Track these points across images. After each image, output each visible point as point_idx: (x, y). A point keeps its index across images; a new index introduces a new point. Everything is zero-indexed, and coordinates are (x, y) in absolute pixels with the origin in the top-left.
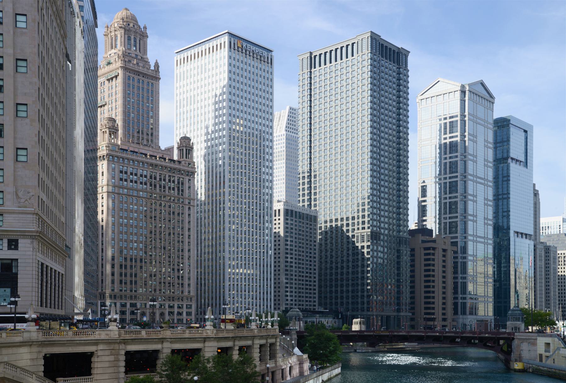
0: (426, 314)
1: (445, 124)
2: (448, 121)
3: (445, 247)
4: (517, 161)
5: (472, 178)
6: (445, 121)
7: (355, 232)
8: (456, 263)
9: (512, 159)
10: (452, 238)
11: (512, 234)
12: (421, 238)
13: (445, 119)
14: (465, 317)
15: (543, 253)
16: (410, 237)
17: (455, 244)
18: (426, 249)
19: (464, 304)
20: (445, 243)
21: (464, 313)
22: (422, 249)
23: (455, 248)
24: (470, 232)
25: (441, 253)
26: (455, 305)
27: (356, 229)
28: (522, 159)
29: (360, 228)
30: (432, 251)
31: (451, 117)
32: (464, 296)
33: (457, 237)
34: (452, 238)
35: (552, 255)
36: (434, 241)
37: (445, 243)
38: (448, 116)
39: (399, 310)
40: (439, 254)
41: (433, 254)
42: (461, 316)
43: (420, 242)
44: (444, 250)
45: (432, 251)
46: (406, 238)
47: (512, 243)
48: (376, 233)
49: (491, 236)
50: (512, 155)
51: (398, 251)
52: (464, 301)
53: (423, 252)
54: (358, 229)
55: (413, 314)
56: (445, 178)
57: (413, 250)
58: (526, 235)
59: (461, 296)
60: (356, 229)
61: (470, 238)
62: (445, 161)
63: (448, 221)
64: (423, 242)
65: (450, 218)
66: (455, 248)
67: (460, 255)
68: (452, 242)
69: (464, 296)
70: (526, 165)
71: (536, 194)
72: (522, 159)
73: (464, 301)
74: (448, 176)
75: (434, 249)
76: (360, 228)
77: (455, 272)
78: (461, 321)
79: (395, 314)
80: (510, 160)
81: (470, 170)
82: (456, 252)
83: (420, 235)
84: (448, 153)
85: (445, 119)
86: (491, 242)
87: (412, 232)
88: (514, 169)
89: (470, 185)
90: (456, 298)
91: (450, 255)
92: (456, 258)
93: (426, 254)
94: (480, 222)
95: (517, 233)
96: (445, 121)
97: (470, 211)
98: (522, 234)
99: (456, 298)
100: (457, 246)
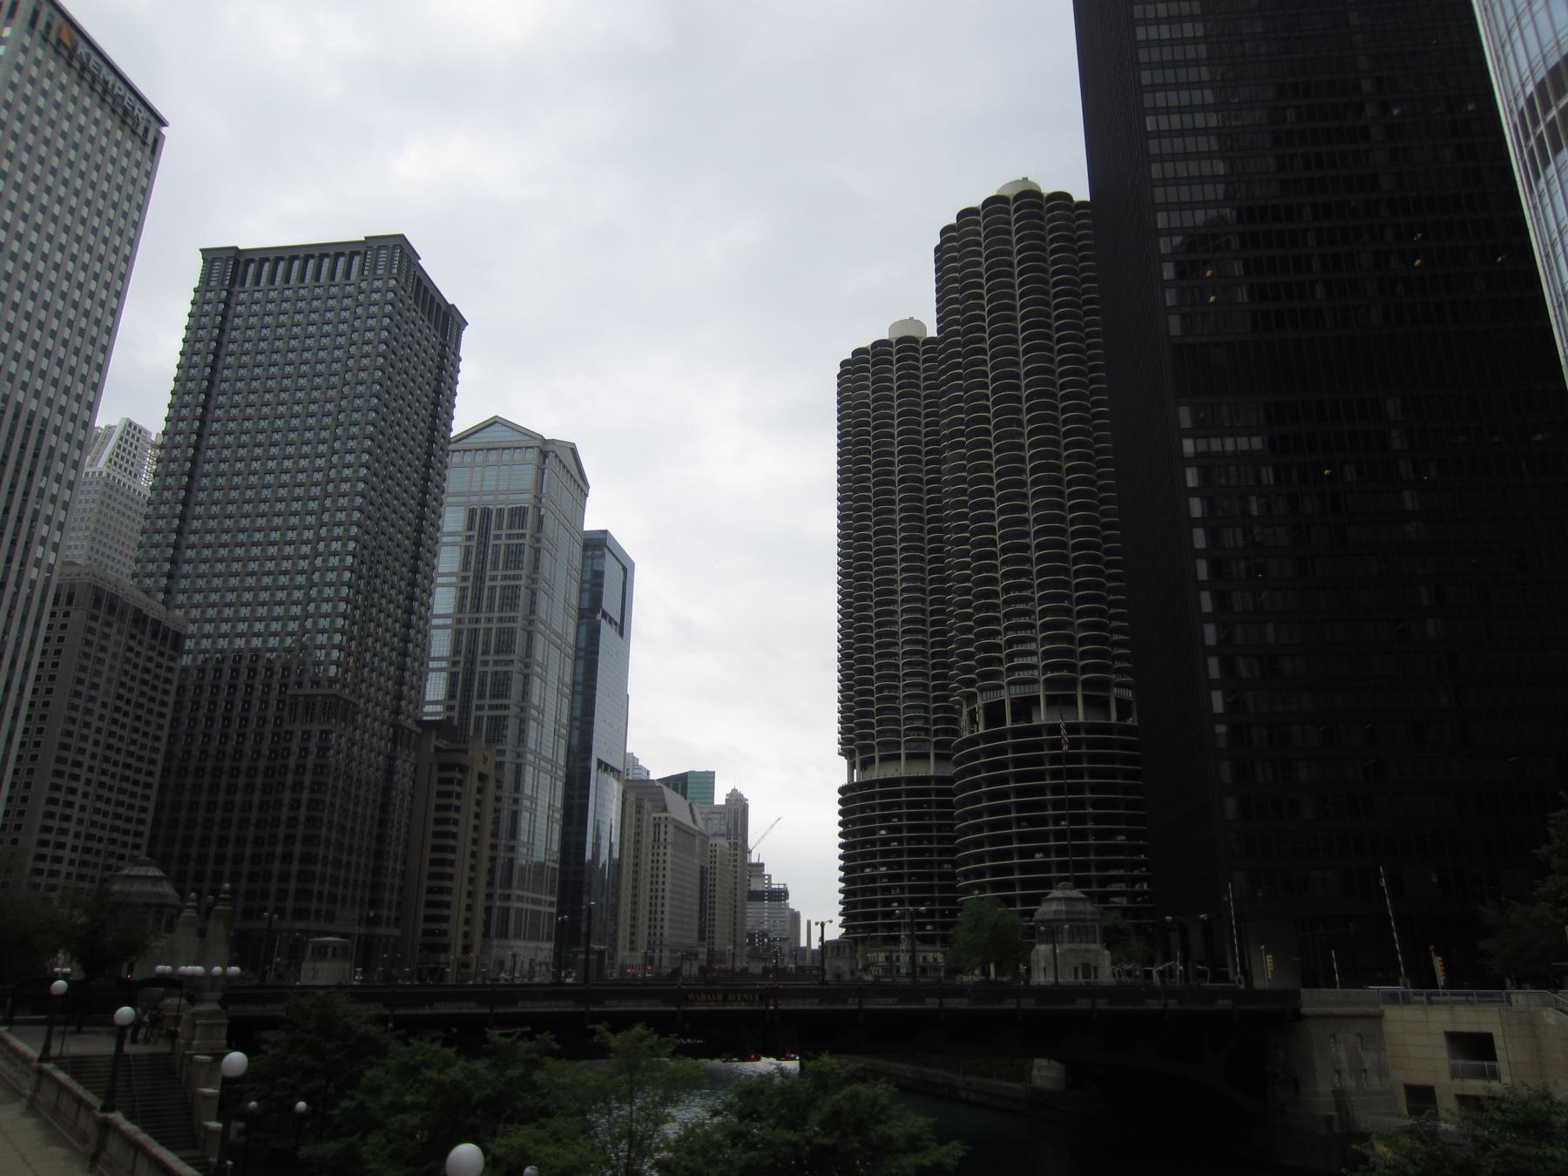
3: (485, 771)
4: (611, 621)
9: (605, 615)
11: (594, 765)
14: (504, 942)
18: (443, 767)
19: (505, 912)
20: (485, 758)
21: (503, 934)
24: (531, 745)
26: (488, 910)
28: (617, 619)
32: (507, 892)
33: (501, 753)
37: (485, 758)
39: (373, 922)
40: (472, 782)
41: (460, 783)
42: (495, 942)
44: (482, 777)
45: (458, 775)
46: (411, 731)
48: (347, 702)
49: (562, 761)
50: (605, 606)
51: (391, 758)
52: (506, 904)
54: (300, 684)
56: (489, 620)
58: (613, 769)
59: (499, 891)
61: (530, 757)
63: (486, 713)
64: (437, 749)
65: (491, 707)
69: (507, 892)
70: (621, 634)
72: (617, 619)
74: (496, 615)
78: (495, 953)
80: (599, 616)
86: (561, 773)
89: (540, 645)
90: (489, 896)
92: (498, 799)
93: (442, 781)
95: (600, 763)
97: (535, 700)
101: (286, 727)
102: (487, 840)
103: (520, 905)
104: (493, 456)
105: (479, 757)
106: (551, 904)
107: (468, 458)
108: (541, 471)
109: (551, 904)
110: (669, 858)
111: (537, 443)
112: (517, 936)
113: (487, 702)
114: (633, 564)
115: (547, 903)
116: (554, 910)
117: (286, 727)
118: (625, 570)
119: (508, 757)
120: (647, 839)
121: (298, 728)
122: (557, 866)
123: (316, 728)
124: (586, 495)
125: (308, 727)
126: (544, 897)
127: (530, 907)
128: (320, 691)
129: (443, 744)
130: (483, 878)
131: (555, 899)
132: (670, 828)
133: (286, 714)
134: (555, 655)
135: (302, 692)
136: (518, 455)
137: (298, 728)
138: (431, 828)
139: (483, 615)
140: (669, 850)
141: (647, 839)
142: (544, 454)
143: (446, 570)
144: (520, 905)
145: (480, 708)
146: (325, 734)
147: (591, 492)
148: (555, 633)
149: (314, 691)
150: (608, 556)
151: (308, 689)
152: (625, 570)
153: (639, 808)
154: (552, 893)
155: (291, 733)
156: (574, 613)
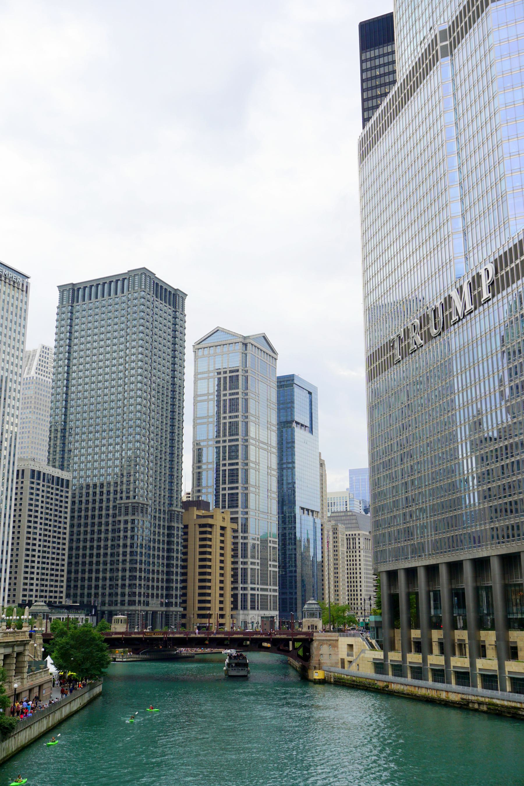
0: (200, 609)
1: (225, 378)
2: (228, 375)
3: (223, 525)
4: (302, 425)
5: (254, 442)
6: (225, 375)
7: (118, 502)
8: (235, 544)
9: (297, 423)
10: (232, 513)
12: (196, 512)
13: (225, 372)
14: (246, 612)
15: (331, 533)
16: (183, 511)
17: (234, 520)
18: (201, 526)
20: (224, 518)
21: (244, 608)
22: (197, 526)
23: (235, 526)
25: (219, 531)
26: (235, 596)
27: (118, 498)
29: (124, 497)
30: (209, 529)
31: (231, 372)
33: (237, 512)
34: (232, 513)
35: (340, 536)
36: (212, 517)
37: (224, 518)
38: (228, 370)
39: (168, 605)
40: (217, 531)
42: (241, 612)
43: (195, 517)
44: (223, 528)
45: (209, 529)
47: (298, 521)
48: (143, 504)
53: (198, 530)
54: (121, 498)
55: (185, 609)
56: (224, 441)
57: (186, 527)
60: (118, 498)
62: (225, 421)
64: (198, 516)
66: (235, 526)
67: (240, 535)
68: (232, 519)
70: (311, 431)
71: (322, 465)
72: (308, 424)
73: (245, 592)
74: (227, 438)
75: (211, 526)
76: (124, 497)
77: (235, 556)
78: (241, 618)
79: (164, 609)
80: (294, 424)
81: (252, 433)
82: (235, 531)
83: (195, 508)
84: (228, 412)
85: (225, 372)
87: (187, 505)
88: (299, 434)
89: (252, 450)
90: (235, 589)
91: (229, 533)
93: (201, 533)
94: (263, 494)
95: (303, 509)
96: (225, 375)
98: (308, 510)
99: (235, 588)
100: (237, 523)
101: (118, 518)
102: (229, 560)
103: (253, 592)
104: (219, 349)
105: (220, 518)
106: (275, 590)
107: (206, 351)
108: (245, 355)
109: (275, 590)
110: (362, 558)
111: (241, 340)
112: (253, 608)
113: (227, 486)
114: (316, 388)
115: (272, 591)
116: (277, 594)
117: (118, 518)
118: (310, 393)
119: (240, 516)
120: (342, 549)
121: (122, 518)
122: (277, 570)
123: (129, 518)
124: (276, 359)
125: (126, 518)
126: (269, 587)
127: (260, 593)
128: (130, 501)
129: (202, 512)
130: (228, 579)
131: (277, 588)
132: (362, 540)
133: (117, 512)
134: (263, 454)
135: (122, 502)
136: (232, 347)
137: (122, 518)
138: (198, 557)
139: (221, 439)
140: (362, 553)
141: (342, 549)
142: (245, 345)
143: (201, 416)
144: (253, 592)
145: (224, 489)
146: (133, 521)
147: (279, 357)
148: (263, 443)
149: (127, 501)
150: (296, 390)
151: (124, 501)
152: (310, 393)
153: (335, 531)
154: (275, 585)
155: (120, 521)
156: (275, 428)
